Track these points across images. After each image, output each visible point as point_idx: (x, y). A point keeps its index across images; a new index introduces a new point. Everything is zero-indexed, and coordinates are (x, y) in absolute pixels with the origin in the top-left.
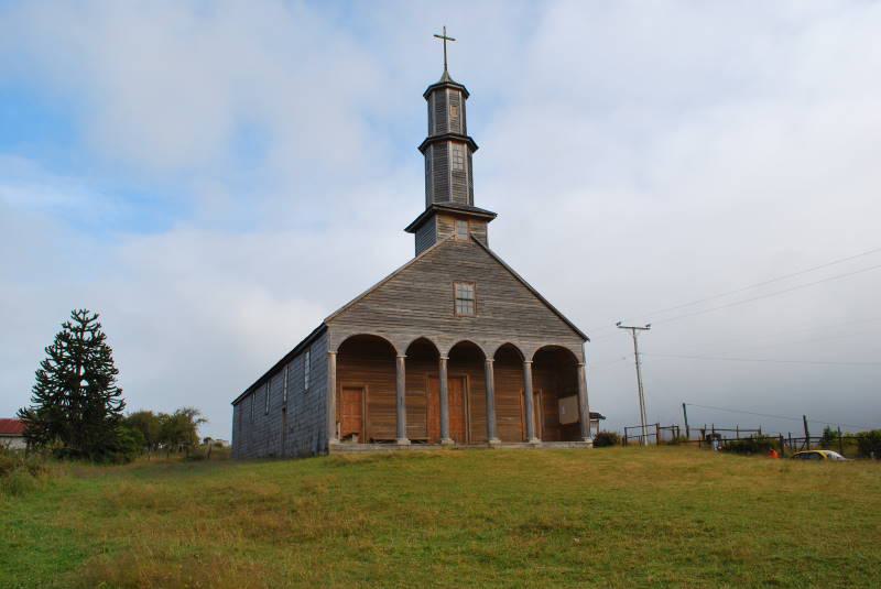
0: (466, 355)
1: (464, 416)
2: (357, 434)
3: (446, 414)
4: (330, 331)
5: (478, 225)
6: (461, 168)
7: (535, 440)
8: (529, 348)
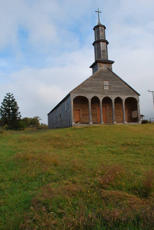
1: (107, 116)
2: (79, 121)
3: (102, 116)
4: (71, 95)
5: (109, 65)
6: (104, 49)
7: (125, 122)
8: (124, 98)
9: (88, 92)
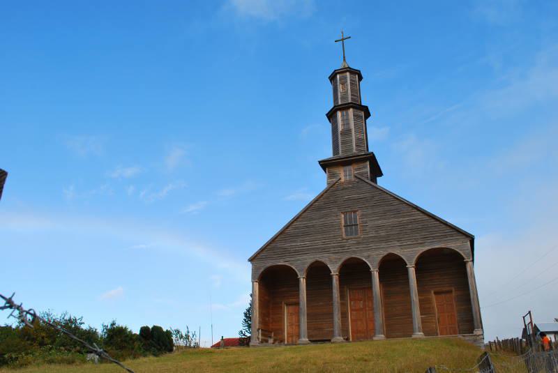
0: (354, 272)
8: (410, 255)
9: (296, 251)
